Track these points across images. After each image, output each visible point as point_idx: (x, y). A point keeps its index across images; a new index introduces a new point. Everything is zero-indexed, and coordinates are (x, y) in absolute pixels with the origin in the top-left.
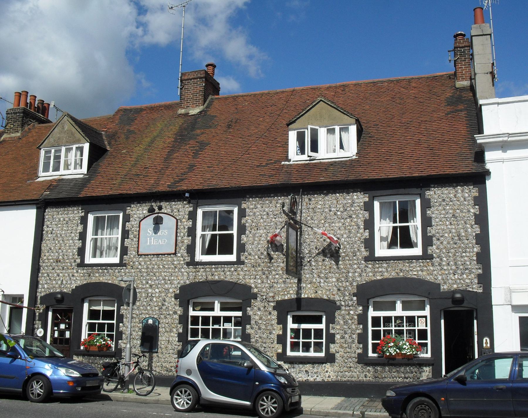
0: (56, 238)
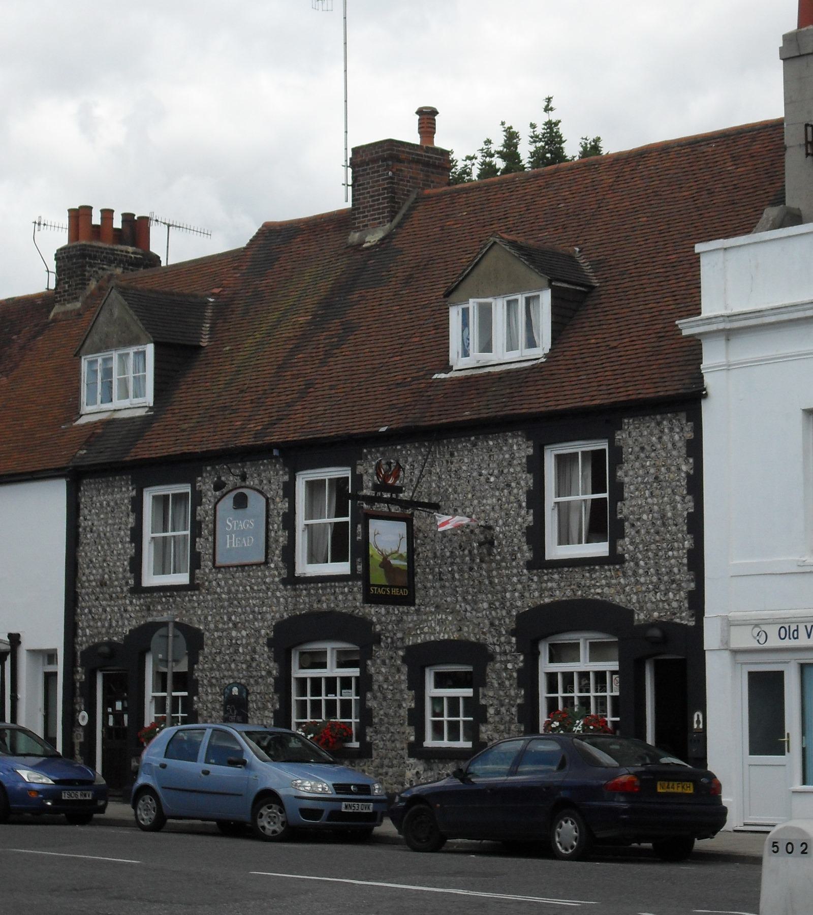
0: (97, 541)
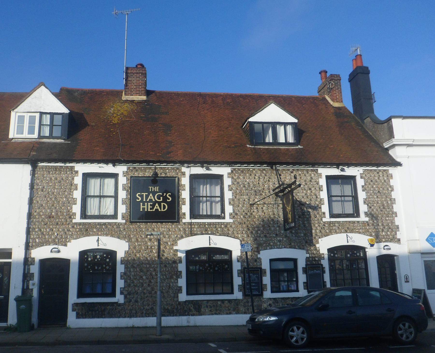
0: (47, 196)
